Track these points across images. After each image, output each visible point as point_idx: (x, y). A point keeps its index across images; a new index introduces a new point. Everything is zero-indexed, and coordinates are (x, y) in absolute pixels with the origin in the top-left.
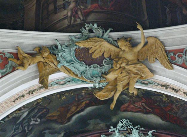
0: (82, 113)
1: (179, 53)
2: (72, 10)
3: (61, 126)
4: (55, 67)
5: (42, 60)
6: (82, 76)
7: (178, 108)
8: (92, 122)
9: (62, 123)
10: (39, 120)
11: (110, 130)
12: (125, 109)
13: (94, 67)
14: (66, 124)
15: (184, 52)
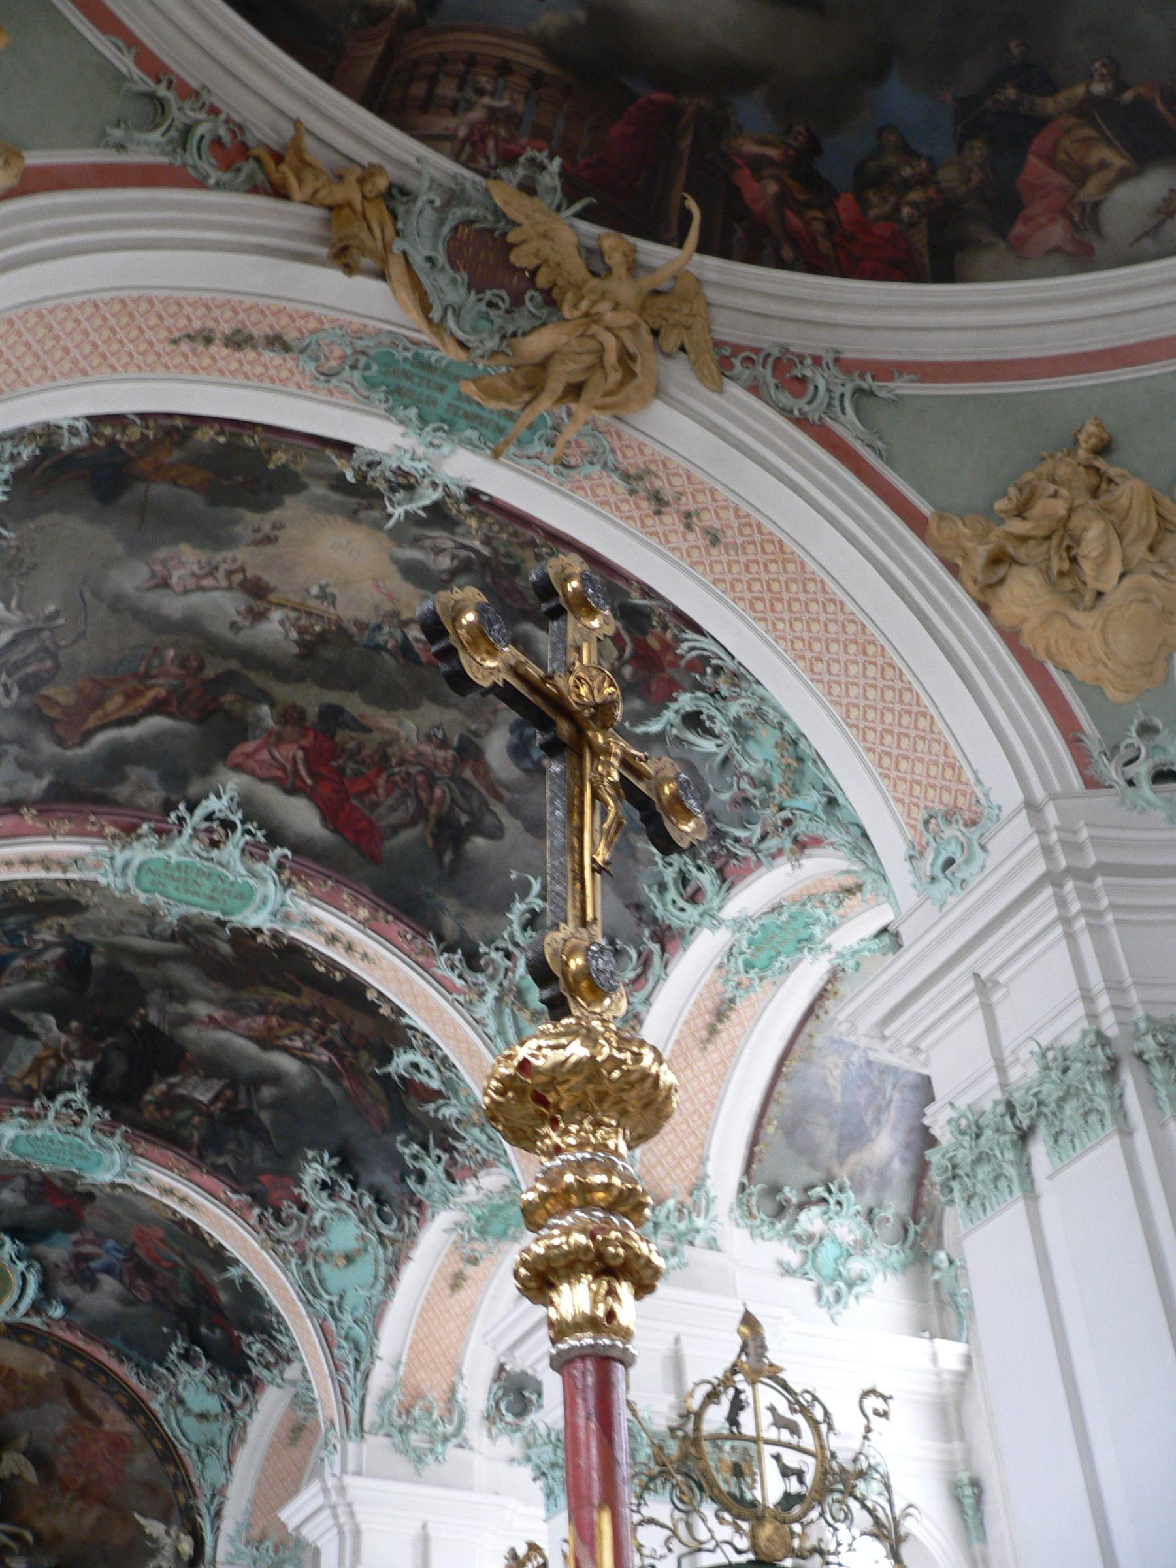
0: (129, 733)
1: (747, 353)
2: (473, 126)
3: (57, 750)
4: (380, 244)
5: (357, 199)
6: (444, 317)
7: (391, 785)
8: (135, 773)
9: (61, 742)
10: (15, 692)
11: (173, 817)
12: (240, 760)
13: (491, 304)
14: (70, 753)
15: (762, 356)
